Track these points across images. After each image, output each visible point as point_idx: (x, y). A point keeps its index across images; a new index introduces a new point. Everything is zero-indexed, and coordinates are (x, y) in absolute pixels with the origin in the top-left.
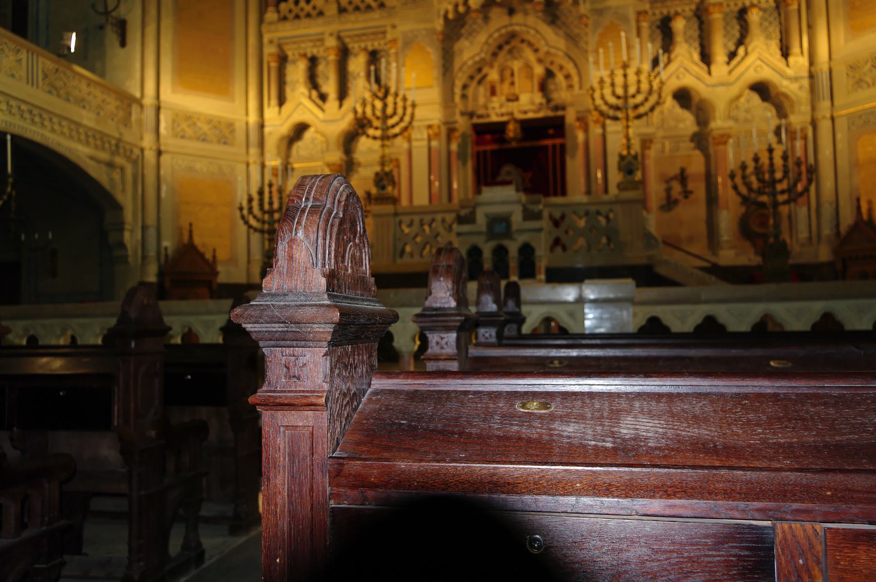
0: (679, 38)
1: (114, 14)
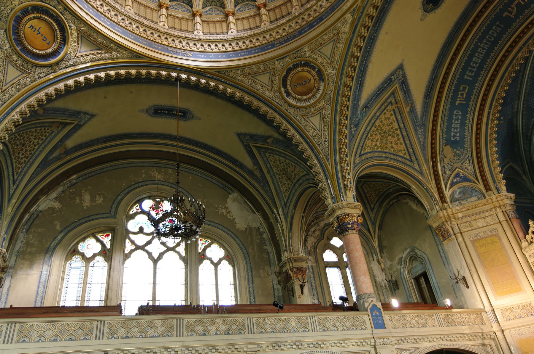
1: (459, 277)
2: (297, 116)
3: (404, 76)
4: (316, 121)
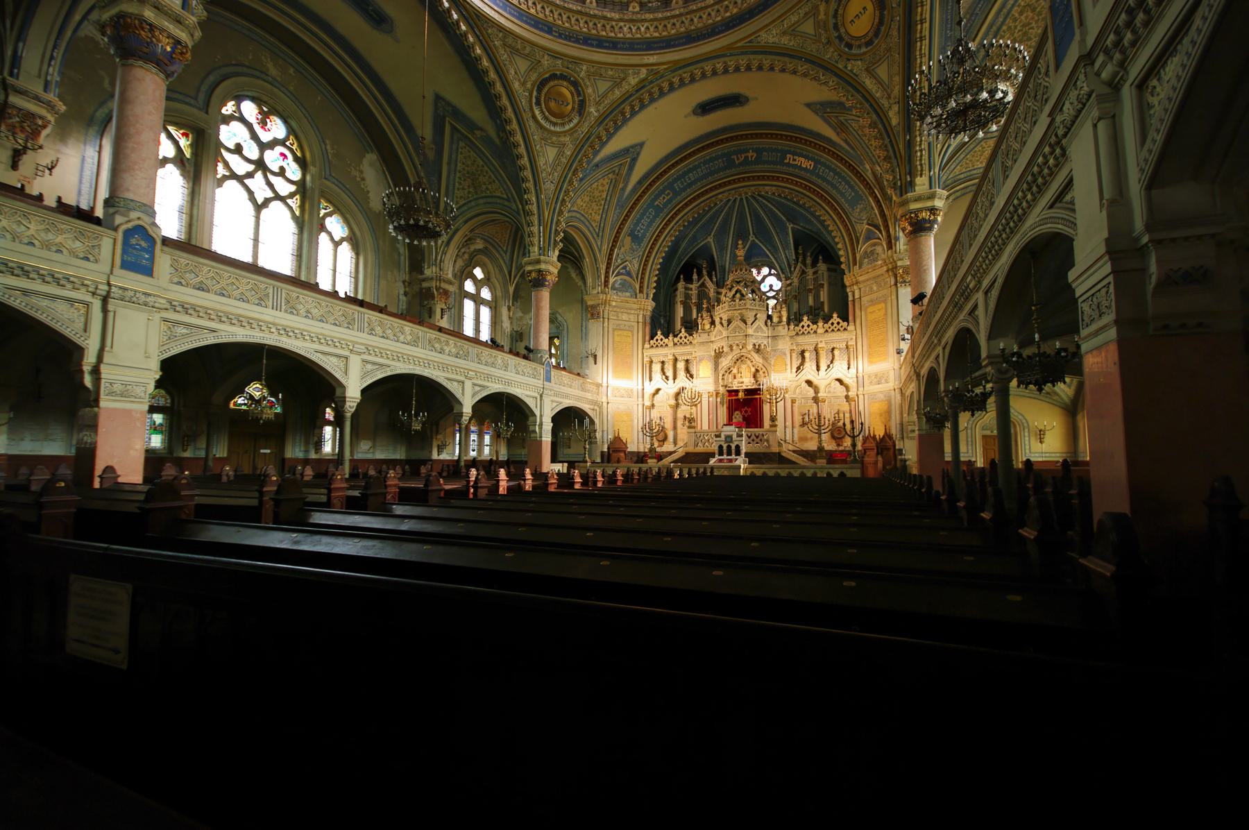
0: (807, 360)
2: (536, 136)
3: (638, 154)
4: (551, 153)
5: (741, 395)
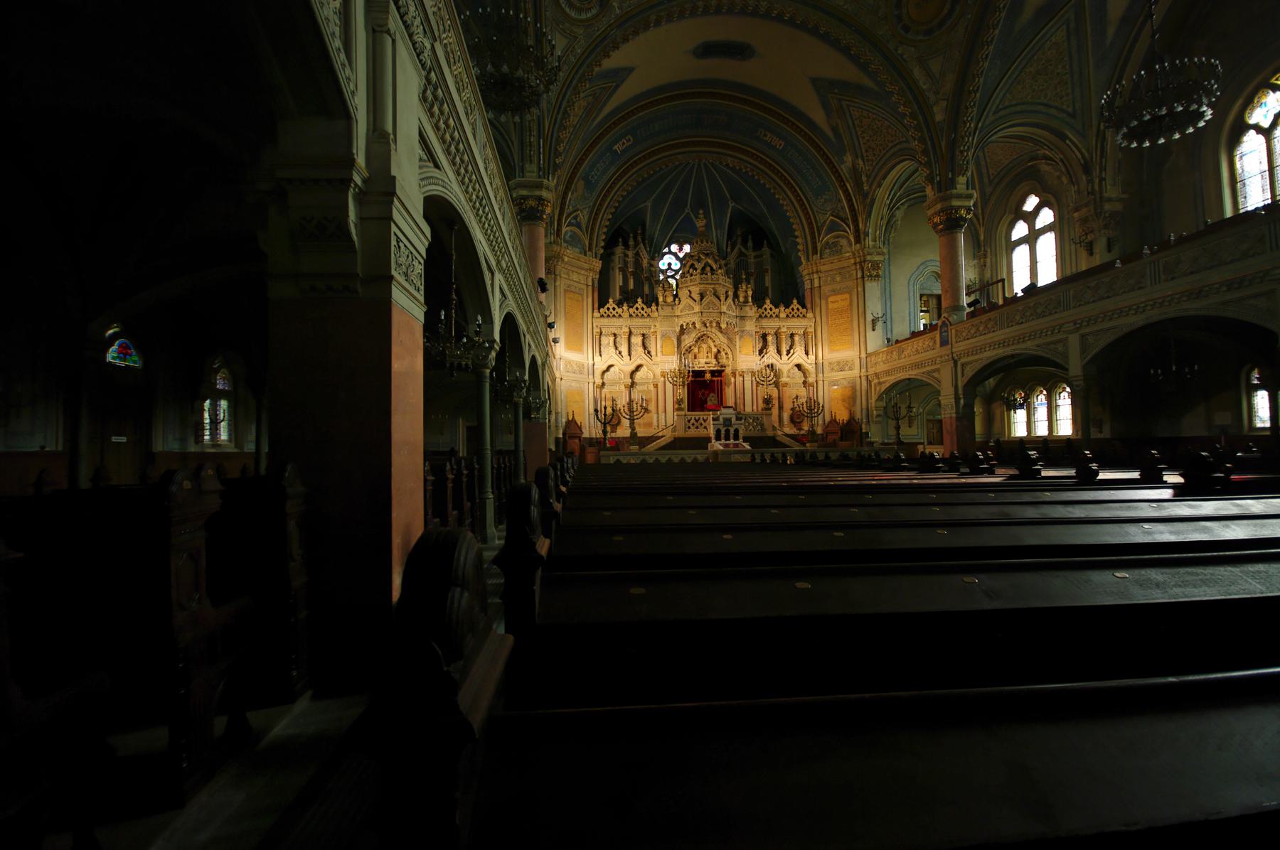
5: (708, 376)
